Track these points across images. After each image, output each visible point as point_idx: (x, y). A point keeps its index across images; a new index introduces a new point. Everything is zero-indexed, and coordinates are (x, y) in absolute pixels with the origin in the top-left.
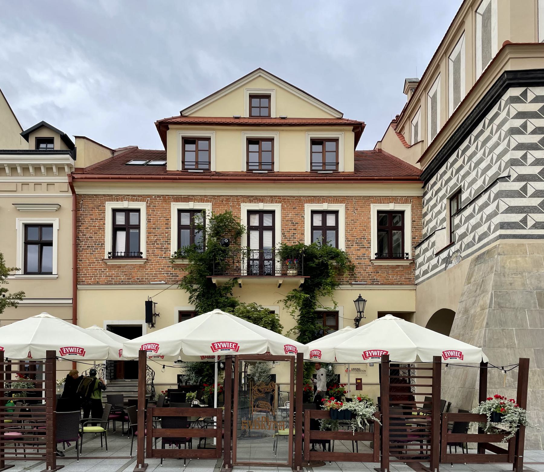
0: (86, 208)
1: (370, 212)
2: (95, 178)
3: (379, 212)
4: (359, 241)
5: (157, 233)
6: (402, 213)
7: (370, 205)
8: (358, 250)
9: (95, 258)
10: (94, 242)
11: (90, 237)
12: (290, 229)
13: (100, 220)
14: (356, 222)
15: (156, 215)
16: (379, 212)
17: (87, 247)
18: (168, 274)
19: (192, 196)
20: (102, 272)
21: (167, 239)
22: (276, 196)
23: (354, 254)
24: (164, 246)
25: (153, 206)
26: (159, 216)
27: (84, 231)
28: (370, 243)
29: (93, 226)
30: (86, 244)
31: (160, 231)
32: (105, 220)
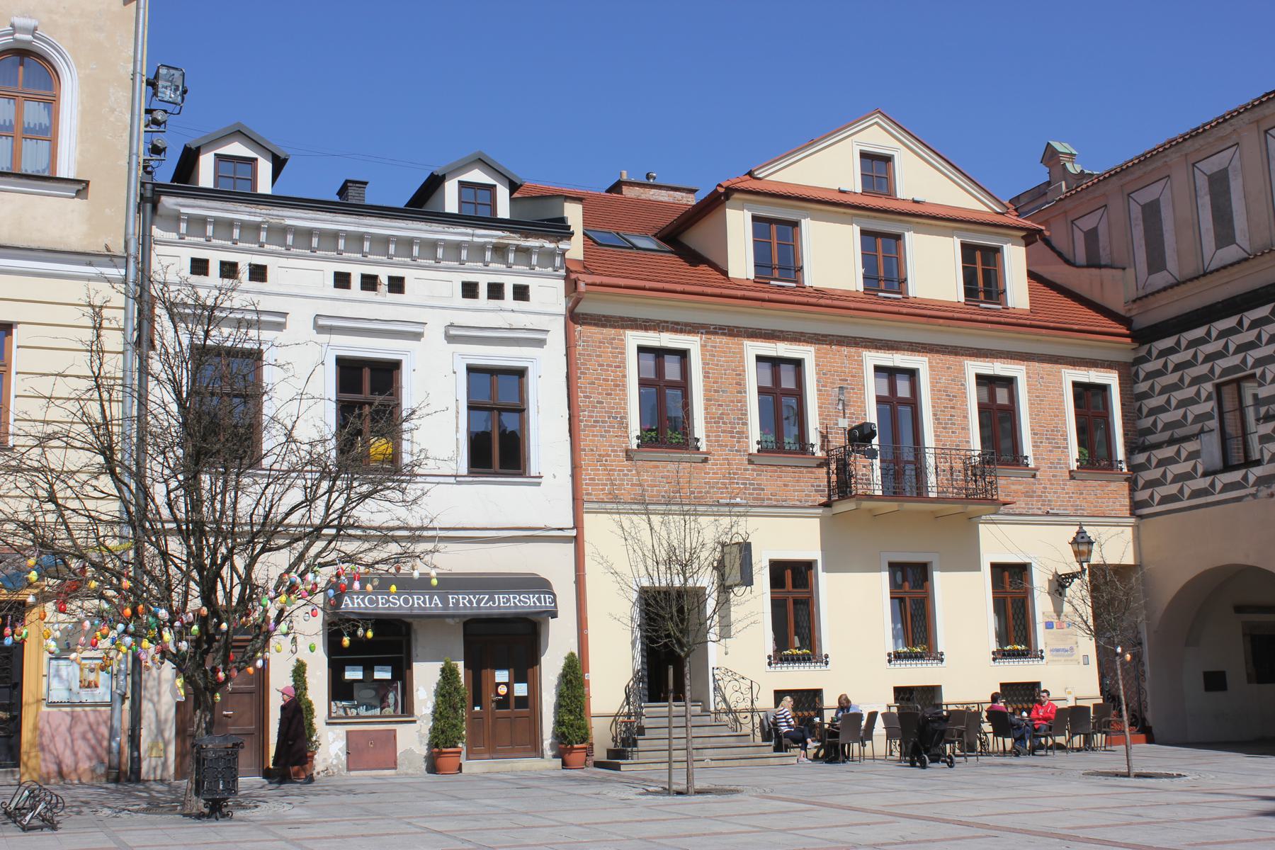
0: (588, 341)
1: (1061, 383)
2: (643, 289)
3: (1076, 385)
4: (1050, 435)
5: (723, 401)
6: (1104, 389)
7: (1061, 372)
8: (1051, 451)
9: (609, 446)
10: (606, 412)
11: (598, 402)
12: (945, 407)
13: (616, 367)
14: (1042, 401)
15: (717, 365)
16: (1076, 385)
17: (595, 422)
18: (746, 484)
19: (779, 331)
20: (625, 475)
21: (742, 414)
22: (919, 343)
23: (1044, 459)
24: (736, 428)
25: (712, 346)
26: (722, 366)
27: (586, 388)
28: (1066, 439)
29: (604, 380)
30: (592, 417)
31: (727, 397)
32: (625, 367)
